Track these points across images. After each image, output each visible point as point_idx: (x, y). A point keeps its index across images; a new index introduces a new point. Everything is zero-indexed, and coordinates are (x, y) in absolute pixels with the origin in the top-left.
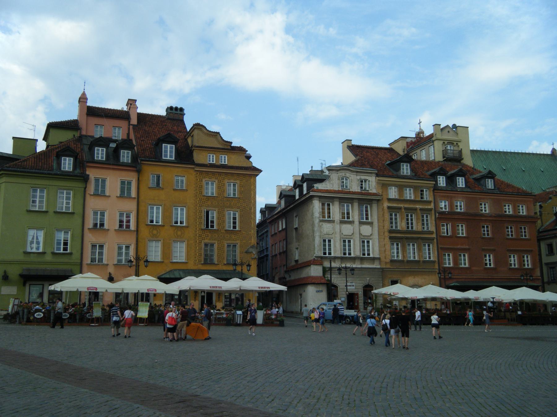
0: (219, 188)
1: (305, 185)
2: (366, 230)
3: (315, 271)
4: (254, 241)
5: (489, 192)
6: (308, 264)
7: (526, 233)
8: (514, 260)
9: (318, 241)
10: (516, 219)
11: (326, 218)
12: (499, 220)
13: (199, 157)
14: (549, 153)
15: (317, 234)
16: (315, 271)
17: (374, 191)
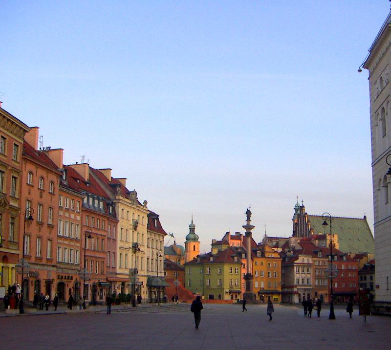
0: (272, 265)
1: (286, 258)
2: (309, 275)
3: (295, 290)
4: (280, 281)
5: (344, 261)
6: (292, 287)
7: (355, 275)
8: (351, 286)
9: (295, 280)
10: (352, 270)
11: (298, 272)
12: (347, 271)
13: (267, 255)
14: (363, 218)
15: (295, 278)
16: (295, 290)
17: (311, 262)
